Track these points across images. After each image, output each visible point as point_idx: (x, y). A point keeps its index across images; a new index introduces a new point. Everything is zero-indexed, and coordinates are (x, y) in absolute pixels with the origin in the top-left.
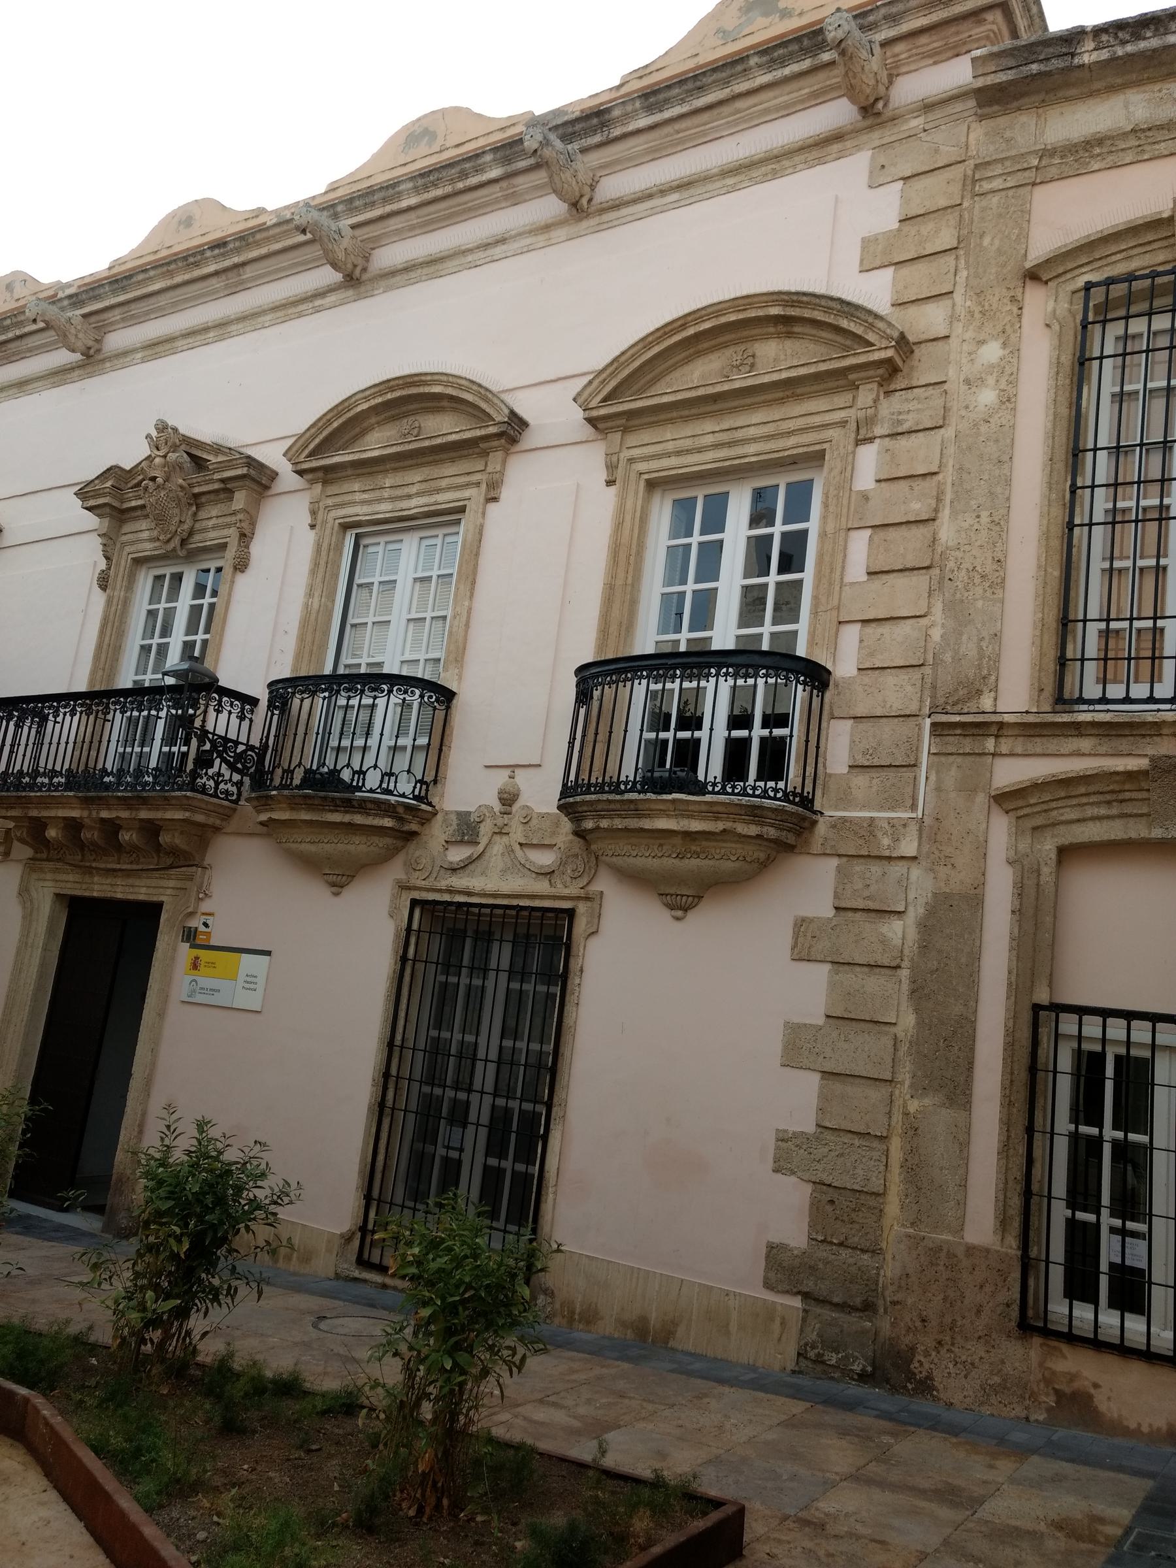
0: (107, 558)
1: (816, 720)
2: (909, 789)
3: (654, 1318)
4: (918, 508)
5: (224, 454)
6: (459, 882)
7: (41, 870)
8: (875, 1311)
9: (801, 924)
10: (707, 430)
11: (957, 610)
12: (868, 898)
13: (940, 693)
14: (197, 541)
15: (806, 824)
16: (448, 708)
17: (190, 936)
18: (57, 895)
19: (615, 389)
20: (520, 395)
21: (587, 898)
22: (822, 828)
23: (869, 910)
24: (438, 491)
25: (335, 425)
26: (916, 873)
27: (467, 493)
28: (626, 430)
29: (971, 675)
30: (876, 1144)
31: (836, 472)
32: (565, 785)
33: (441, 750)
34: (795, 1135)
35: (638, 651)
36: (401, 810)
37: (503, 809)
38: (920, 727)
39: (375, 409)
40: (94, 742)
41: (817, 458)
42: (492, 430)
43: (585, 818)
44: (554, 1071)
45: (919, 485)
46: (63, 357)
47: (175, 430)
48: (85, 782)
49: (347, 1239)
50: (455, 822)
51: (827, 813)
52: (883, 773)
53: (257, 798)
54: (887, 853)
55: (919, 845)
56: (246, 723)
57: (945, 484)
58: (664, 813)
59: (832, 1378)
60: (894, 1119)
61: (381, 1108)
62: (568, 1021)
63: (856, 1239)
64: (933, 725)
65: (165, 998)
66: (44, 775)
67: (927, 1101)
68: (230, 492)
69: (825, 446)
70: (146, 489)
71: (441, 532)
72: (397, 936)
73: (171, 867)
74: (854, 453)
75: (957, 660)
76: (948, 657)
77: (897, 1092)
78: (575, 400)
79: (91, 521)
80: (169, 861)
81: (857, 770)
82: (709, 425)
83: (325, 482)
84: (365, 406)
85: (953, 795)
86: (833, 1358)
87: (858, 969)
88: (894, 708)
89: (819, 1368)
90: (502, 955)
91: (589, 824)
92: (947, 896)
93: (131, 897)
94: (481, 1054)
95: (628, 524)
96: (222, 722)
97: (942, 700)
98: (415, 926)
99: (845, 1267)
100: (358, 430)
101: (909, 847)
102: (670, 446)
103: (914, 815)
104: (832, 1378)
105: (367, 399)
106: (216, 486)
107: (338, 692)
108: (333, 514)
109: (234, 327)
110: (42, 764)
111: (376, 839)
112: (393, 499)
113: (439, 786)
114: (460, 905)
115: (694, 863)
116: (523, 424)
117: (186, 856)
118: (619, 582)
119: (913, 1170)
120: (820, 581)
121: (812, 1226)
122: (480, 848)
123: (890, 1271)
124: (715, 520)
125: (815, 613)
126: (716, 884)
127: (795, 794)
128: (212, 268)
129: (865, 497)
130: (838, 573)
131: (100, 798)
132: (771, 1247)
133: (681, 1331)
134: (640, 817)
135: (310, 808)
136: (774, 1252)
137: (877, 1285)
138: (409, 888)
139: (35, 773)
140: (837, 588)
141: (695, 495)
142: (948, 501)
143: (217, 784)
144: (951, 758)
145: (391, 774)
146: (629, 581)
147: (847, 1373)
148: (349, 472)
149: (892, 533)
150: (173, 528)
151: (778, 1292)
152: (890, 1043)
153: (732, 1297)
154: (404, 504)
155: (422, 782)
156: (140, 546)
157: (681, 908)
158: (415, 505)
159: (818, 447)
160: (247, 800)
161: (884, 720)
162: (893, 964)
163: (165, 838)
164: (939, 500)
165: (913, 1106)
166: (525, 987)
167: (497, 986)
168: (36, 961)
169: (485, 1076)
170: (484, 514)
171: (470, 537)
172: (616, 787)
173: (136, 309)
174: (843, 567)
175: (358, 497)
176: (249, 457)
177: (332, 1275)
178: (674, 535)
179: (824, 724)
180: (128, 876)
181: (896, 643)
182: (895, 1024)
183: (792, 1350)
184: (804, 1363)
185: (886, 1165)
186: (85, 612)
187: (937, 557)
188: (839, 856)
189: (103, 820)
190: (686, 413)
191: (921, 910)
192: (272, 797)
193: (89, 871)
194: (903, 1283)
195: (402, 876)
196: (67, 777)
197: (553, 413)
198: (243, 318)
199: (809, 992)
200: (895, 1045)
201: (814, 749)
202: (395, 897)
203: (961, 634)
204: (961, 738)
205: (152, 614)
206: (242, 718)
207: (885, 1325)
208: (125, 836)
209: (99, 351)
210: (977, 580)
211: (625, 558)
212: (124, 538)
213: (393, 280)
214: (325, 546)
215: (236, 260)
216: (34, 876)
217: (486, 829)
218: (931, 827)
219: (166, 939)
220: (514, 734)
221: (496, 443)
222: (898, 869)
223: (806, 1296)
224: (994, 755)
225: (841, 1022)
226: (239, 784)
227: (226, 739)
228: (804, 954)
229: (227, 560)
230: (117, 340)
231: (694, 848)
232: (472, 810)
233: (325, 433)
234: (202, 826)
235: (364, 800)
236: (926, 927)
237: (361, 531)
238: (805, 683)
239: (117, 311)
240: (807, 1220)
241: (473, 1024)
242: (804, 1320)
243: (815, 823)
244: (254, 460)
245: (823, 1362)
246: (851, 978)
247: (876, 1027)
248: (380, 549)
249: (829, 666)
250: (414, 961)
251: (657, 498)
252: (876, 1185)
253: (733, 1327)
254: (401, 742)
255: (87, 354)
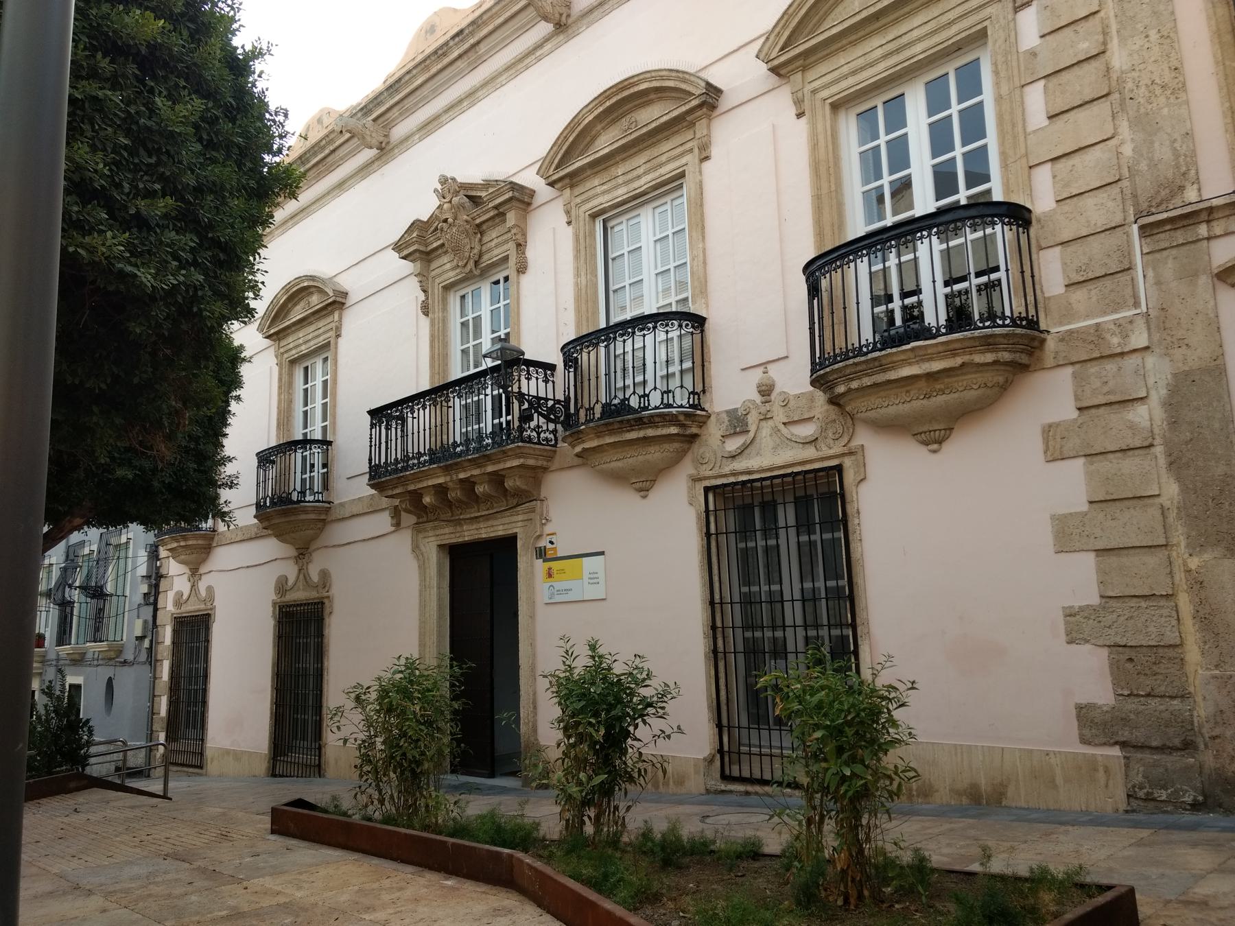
0: (424, 291)
1: (1024, 256)
2: (1129, 291)
3: (983, 783)
4: (1086, 46)
5: (493, 186)
6: (739, 465)
7: (425, 530)
8: (1196, 748)
9: (1049, 431)
10: (875, 45)
11: (1145, 124)
12: (1108, 393)
13: (1141, 199)
14: (486, 260)
15: (1036, 344)
16: (702, 331)
17: (541, 553)
18: (439, 546)
19: (789, 38)
20: (712, 70)
21: (851, 453)
22: (1051, 344)
23: (1111, 404)
24: (661, 165)
25: (571, 139)
26: (1150, 360)
27: (683, 161)
28: (804, 69)
29: (1170, 175)
30: (1163, 602)
31: (1000, 42)
32: (813, 363)
33: (703, 366)
34: (1082, 609)
35: (850, 237)
36: (681, 418)
37: (764, 399)
38: (1128, 234)
39: (598, 118)
40: (442, 426)
41: (980, 37)
42: (695, 103)
43: (836, 385)
44: (852, 598)
45: (1083, 28)
46: (367, 154)
47: (454, 179)
48: (442, 455)
49: (710, 761)
50: (726, 419)
51: (1053, 330)
52: (1100, 283)
53: (570, 435)
54: (1119, 350)
55: (1150, 335)
56: (550, 385)
57: (1108, 18)
58: (906, 362)
59: (1166, 812)
60: (1177, 578)
61: (715, 654)
62: (855, 555)
63: (1163, 688)
64: (1142, 228)
65: (532, 604)
66: (413, 458)
67: (1206, 556)
68: (503, 214)
69: (985, 24)
70: (442, 230)
71: (668, 199)
72: (699, 518)
73: (518, 505)
74: (1014, 19)
75: (1153, 165)
76: (1143, 166)
77: (1174, 554)
78: (757, 57)
79: (408, 267)
80: (515, 502)
81: (1071, 289)
82: (876, 41)
83: (572, 186)
84: (591, 118)
85: (1175, 284)
86: (1163, 795)
87: (1111, 456)
88: (1099, 224)
89: (1151, 805)
90: (787, 515)
91: (841, 389)
92: (1187, 374)
93: (492, 535)
94: (787, 596)
95: (822, 143)
96: (532, 386)
97: (1145, 206)
98: (711, 507)
99: (1157, 714)
100: (588, 139)
101: (1139, 339)
102: (845, 70)
103: (1138, 311)
104: (1166, 812)
105: (591, 111)
106: (492, 214)
107: (615, 338)
108: (584, 208)
109: (480, 93)
110: (410, 450)
111: (666, 446)
112: (626, 183)
113: (708, 394)
114: (744, 483)
115: (940, 399)
116: (718, 91)
117: (523, 494)
118: (825, 191)
119: (1207, 620)
120: (1004, 138)
121: (1116, 683)
122: (751, 434)
123: (1203, 711)
124: (897, 118)
125: (1005, 166)
126: (963, 415)
127: (1021, 319)
128: (456, 54)
129: (1033, 54)
130: (1020, 126)
131: (456, 464)
132: (1079, 708)
133: (1011, 792)
134: (884, 371)
135: (612, 432)
136: (1085, 714)
137: (1192, 724)
138: (700, 480)
139: (406, 458)
140: (1022, 138)
141: (875, 102)
142: (1114, 32)
143: (539, 434)
144: (1165, 253)
145: (668, 392)
146: (833, 188)
147: (1179, 806)
148: (589, 172)
149: (1065, 76)
150: (467, 254)
151: (1096, 745)
152: (1157, 513)
153: (1052, 755)
154: (636, 184)
155: (693, 393)
156: (445, 276)
157: (936, 442)
158: (644, 182)
159: (979, 27)
160: (564, 440)
161: (1092, 238)
162: (1145, 444)
163: (509, 484)
164: (1105, 33)
165: (1194, 563)
166: (813, 537)
167: (788, 541)
168: (434, 598)
169: (793, 613)
170: (700, 172)
171: (693, 194)
172: (859, 352)
173: (408, 103)
174: (1024, 120)
175: (599, 190)
176: (511, 183)
177: (703, 791)
178: (862, 142)
179: (1034, 257)
180: (488, 520)
181: (1089, 169)
182: (1159, 495)
183: (1121, 794)
184: (1134, 803)
185: (1178, 619)
186: (417, 335)
187: (1114, 83)
188: (1072, 364)
189: (461, 481)
190: (854, 37)
191: (1164, 392)
192: (581, 431)
193: (459, 522)
194: (1219, 719)
195: (692, 471)
196: (430, 455)
197: (741, 75)
198: (485, 84)
199: (1070, 486)
200: (1163, 513)
201: (1029, 278)
202: (691, 489)
203: (1152, 143)
204: (1172, 233)
205: (464, 325)
206: (546, 381)
207: (1208, 759)
208: (480, 489)
209: (388, 143)
210: (1158, 91)
211: (825, 171)
212: (433, 273)
213: (592, 17)
214: (582, 235)
215: (472, 41)
216: (421, 536)
217: (752, 419)
218: (1157, 318)
219: (525, 560)
220: (761, 337)
221: (699, 113)
222: (1131, 362)
223: (1123, 745)
224: (1208, 239)
225: (1104, 505)
226: (555, 432)
227: (538, 398)
228: (1057, 455)
229: (510, 270)
230: (399, 131)
231: (938, 387)
232: (738, 406)
233: (564, 148)
234: (534, 468)
235: (652, 416)
236: (1173, 404)
237: (605, 217)
238: (1010, 224)
239: (395, 110)
240: (1109, 679)
241: (774, 574)
242: (1127, 766)
243: (1043, 341)
244: (516, 184)
245: (1154, 800)
246: (1105, 466)
247: (1141, 502)
248: (624, 226)
249: (1028, 205)
250: (717, 534)
251: (842, 115)
252: (1171, 637)
253: (1059, 780)
254: (671, 370)
255: (381, 149)
